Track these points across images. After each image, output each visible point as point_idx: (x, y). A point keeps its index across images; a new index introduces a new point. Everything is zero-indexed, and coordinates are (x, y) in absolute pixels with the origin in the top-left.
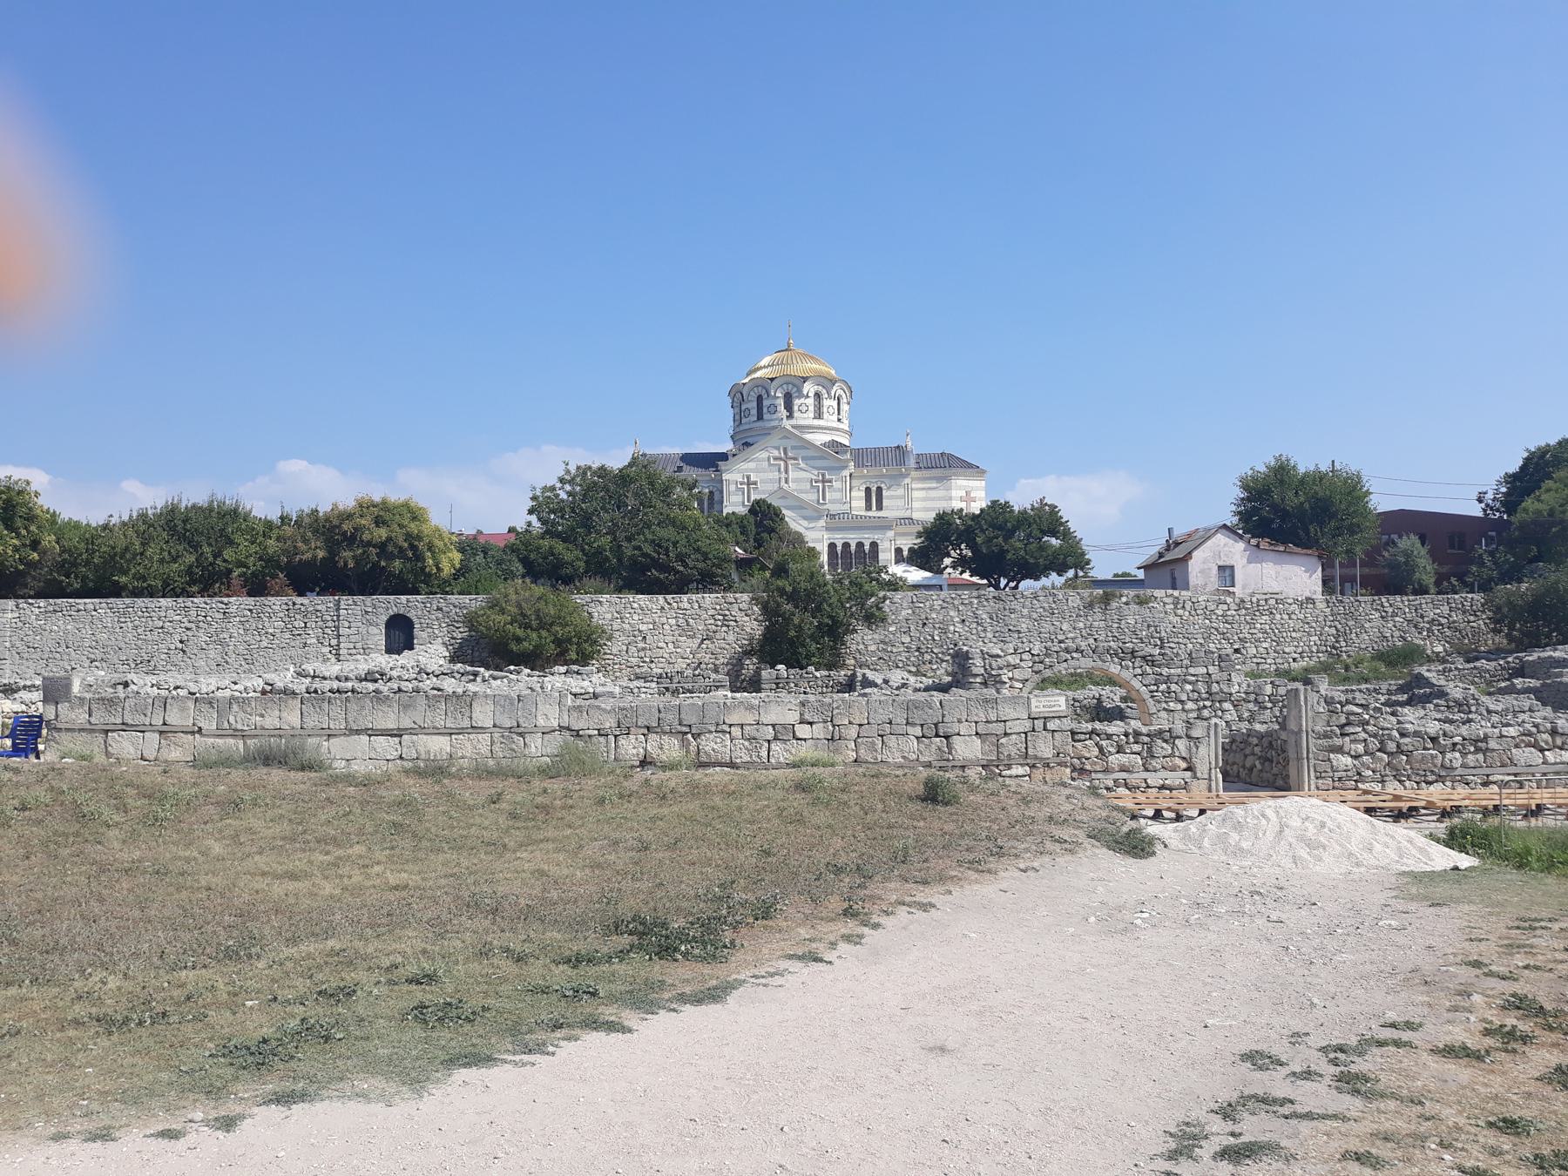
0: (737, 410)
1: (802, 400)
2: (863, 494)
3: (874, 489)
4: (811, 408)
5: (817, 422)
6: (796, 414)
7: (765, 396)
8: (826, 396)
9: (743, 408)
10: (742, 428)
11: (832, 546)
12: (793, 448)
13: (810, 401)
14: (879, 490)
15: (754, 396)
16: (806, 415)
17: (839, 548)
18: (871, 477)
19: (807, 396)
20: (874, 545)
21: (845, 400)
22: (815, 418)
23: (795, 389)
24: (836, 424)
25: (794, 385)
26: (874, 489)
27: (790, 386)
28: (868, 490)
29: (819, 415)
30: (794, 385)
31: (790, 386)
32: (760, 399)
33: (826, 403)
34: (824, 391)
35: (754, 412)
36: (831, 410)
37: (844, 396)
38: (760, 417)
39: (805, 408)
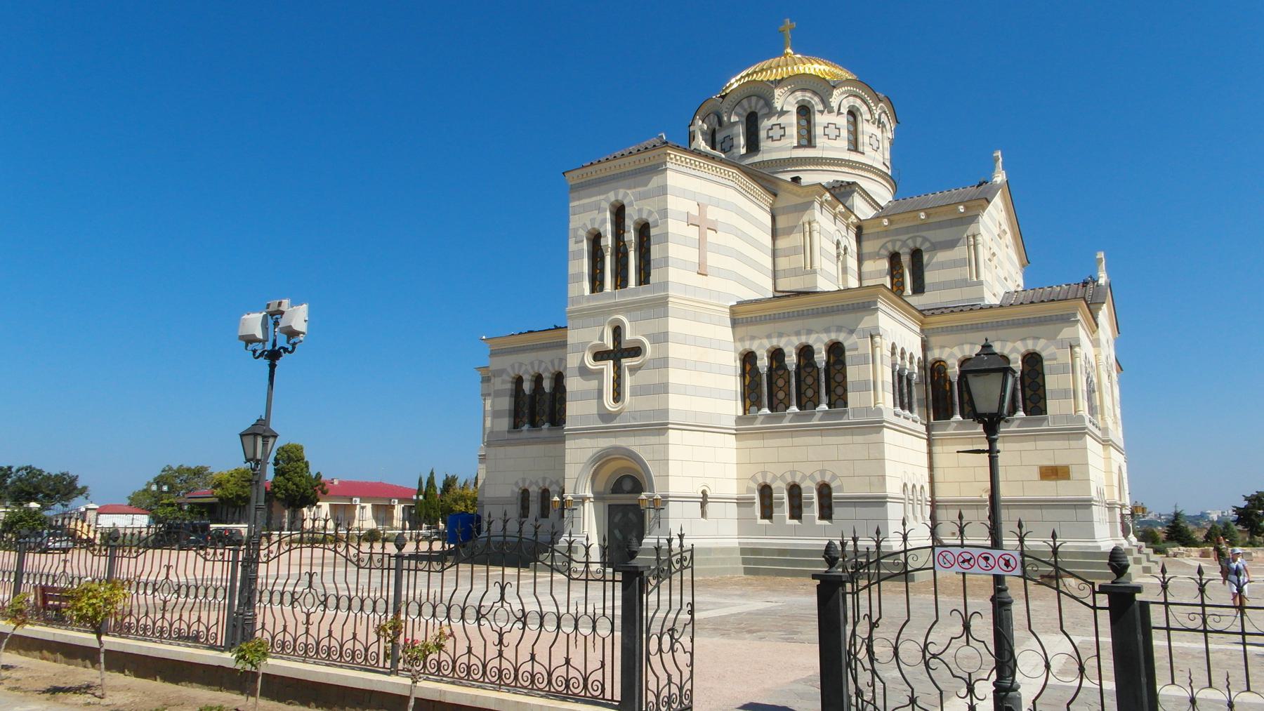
1: (774, 120)
2: (885, 264)
3: (905, 259)
4: (793, 131)
6: (764, 144)
7: (717, 127)
8: (821, 107)
11: (748, 359)
14: (916, 255)
16: (784, 142)
17: (763, 363)
18: (898, 232)
19: (783, 113)
20: (836, 350)
21: (868, 116)
22: (800, 146)
23: (762, 102)
24: (854, 157)
25: (759, 97)
26: (905, 259)
27: (754, 99)
28: (894, 258)
30: (759, 97)
31: (754, 99)
33: (820, 120)
34: (816, 99)
36: (832, 131)
37: (864, 109)
39: (776, 132)
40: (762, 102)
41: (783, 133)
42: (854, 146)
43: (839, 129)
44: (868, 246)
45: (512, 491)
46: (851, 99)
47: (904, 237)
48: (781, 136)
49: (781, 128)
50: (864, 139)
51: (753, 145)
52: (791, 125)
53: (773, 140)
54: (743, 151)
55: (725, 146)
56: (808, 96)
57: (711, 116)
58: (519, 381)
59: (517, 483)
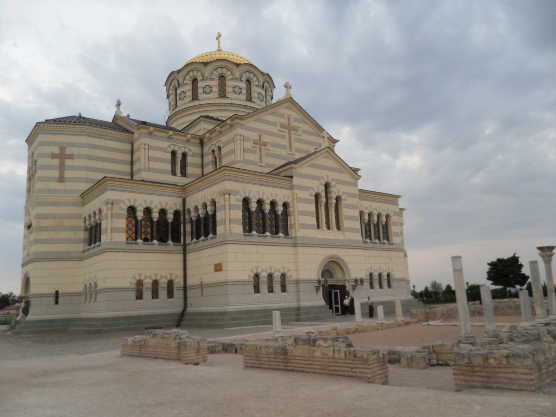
0: (172, 97)
4: (244, 91)
5: (249, 104)
9: (179, 91)
10: (177, 110)
13: (243, 85)
15: (188, 81)
23: (229, 73)
29: (249, 99)
31: (224, 70)
32: (195, 81)
33: (256, 90)
35: (189, 94)
36: (260, 96)
38: (195, 97)
39: (237, 90)
41: (240, 92)
43: (263, 96)
45: (131, 283)
48: (240, 92)
49: (240, 88)
53: (236, 94)
56: (252, 75)
57: (195, 72)
58: (132, 210)
59: (134, 278)
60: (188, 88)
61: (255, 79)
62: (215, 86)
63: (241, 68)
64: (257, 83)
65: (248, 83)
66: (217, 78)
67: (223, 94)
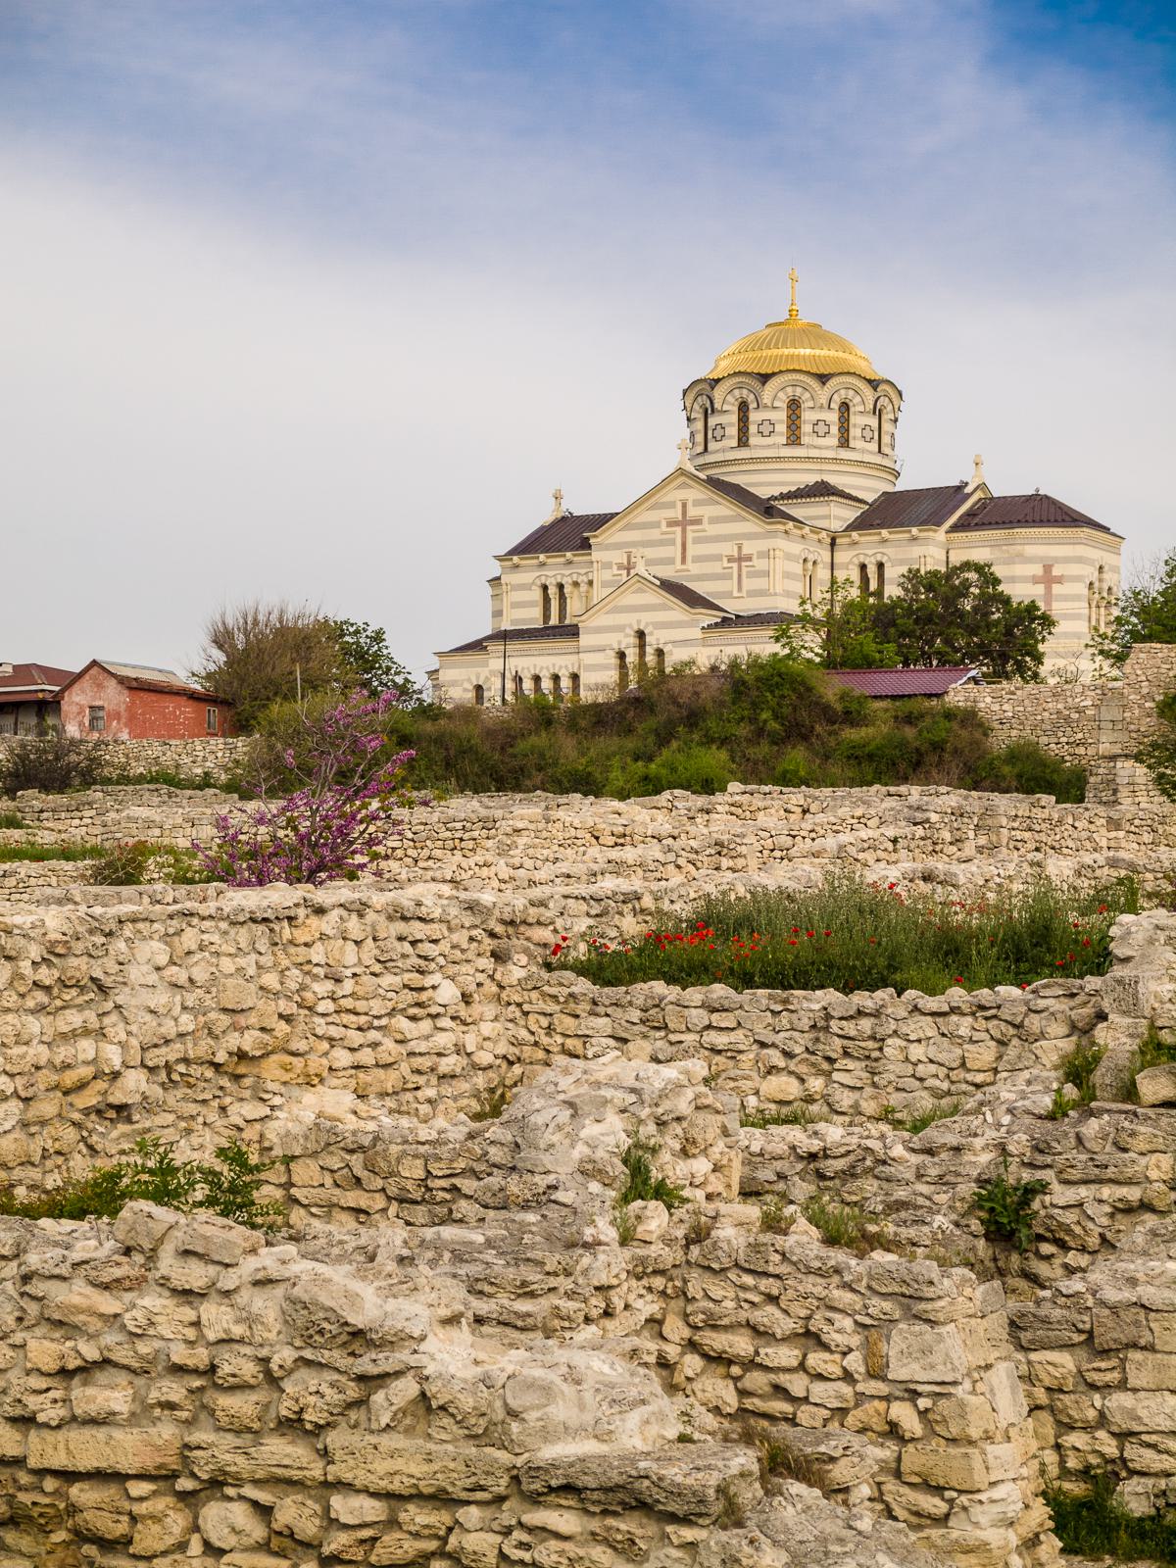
2: (855, 575)
4: (782, 428)
6: (752, 441)
12: (697, 503)
13: (781, 416)
14: (881, 566)
27: (745, 391)
28: (863, 567)
29: (794, 438)
33: (808, 416)
35: (700, 438)
36: (821, 428)
37: (858, 399)
39: (766, 428)
40: (752, 397)
42: (844, 442)
44: (841, 556)
46: (843, 392)
47: (870, 552)
50: (855, 432)
51: (743, 441)
52: (780, 422)
54: (734, 443)
55: (719, 433)
60: (700, 425)
61: (807, 395)
62: (731, 425)
63: (773, 385)
64: (811, 404)
65: (794, 407)
66: (736, 409)
67: (743, 441)
